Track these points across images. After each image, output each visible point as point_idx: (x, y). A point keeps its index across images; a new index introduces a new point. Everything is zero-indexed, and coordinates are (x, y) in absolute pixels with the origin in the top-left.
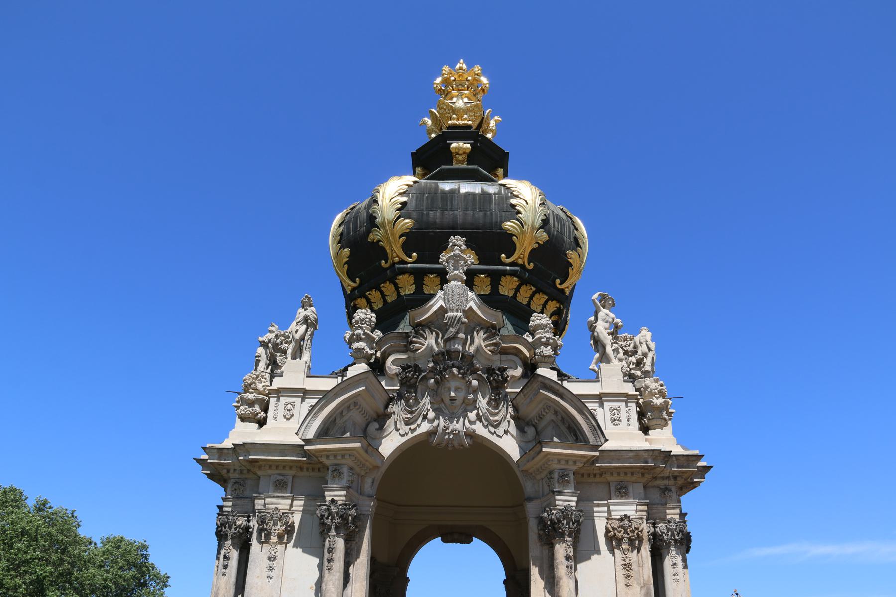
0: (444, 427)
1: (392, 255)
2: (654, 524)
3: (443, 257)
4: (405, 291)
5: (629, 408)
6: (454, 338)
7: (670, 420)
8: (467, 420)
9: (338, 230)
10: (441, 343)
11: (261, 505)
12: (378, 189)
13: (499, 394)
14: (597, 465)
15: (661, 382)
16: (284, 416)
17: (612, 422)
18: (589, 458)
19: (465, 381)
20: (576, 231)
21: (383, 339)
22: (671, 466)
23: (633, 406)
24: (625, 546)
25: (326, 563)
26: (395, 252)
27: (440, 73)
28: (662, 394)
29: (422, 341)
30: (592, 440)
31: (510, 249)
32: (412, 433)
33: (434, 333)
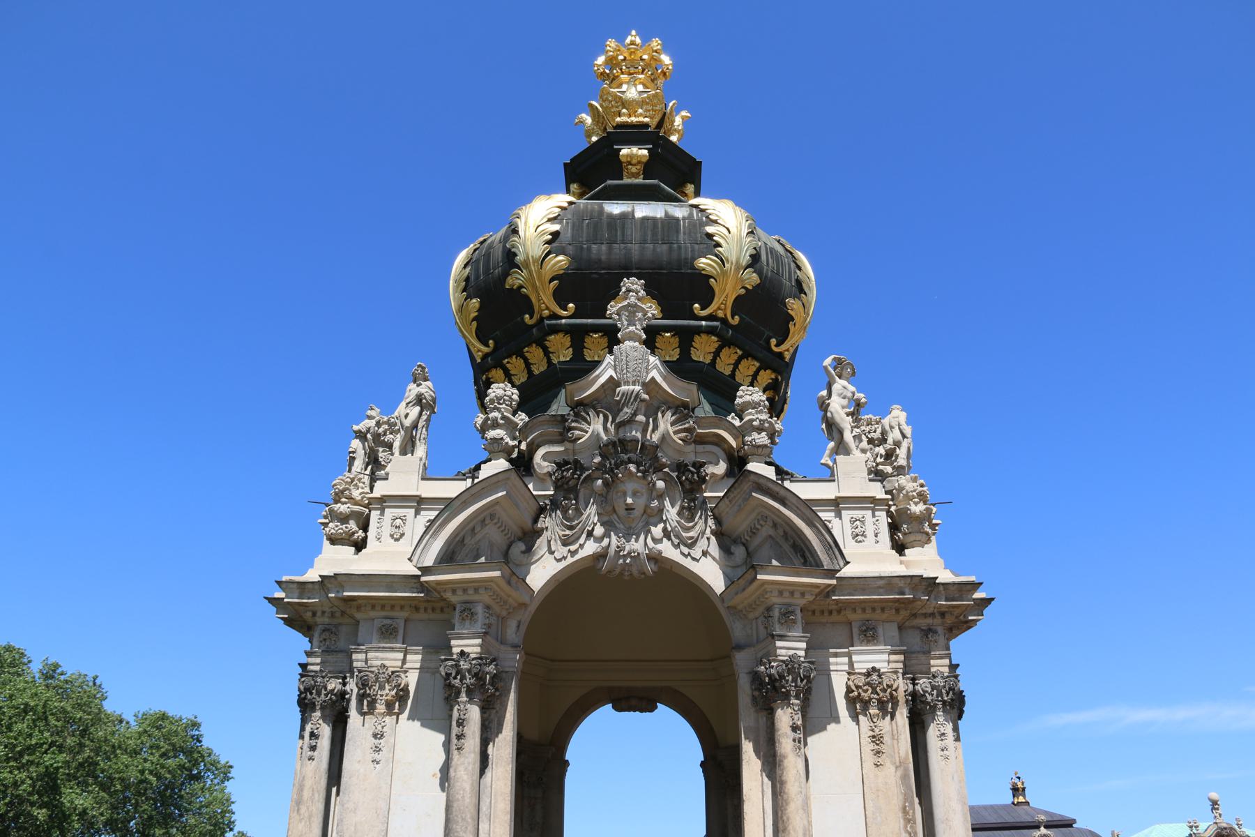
0: (618, 547)
1: (539, 306)
2: (913, 680)
3: (613, 308)
4: (559, 357)
5: (877, 518)
6: (630, 421)
7: (934, 534)
8: (649, 537)
9: (463, 272)
10: (612, 428)
11: (361, 661)
12: (519, 214)
13: (694, 500)
14: (833, 598)
15: (922, 481)
16: (392, 536)
17: (853, 538)
18: (822, 588)
19: (646, 483)
20: (798, 271)
21: (530, 425)
22: (937, 599)
23: (882, 515)
24: (873, 711)
25: (454, 741)
26: (544, 303)
27: (602, 50)
28: (922, 497)
29: (585, 426)
30: (826, 563)
31: (707, 296)
32: (572, 557)
33: (601, 415)
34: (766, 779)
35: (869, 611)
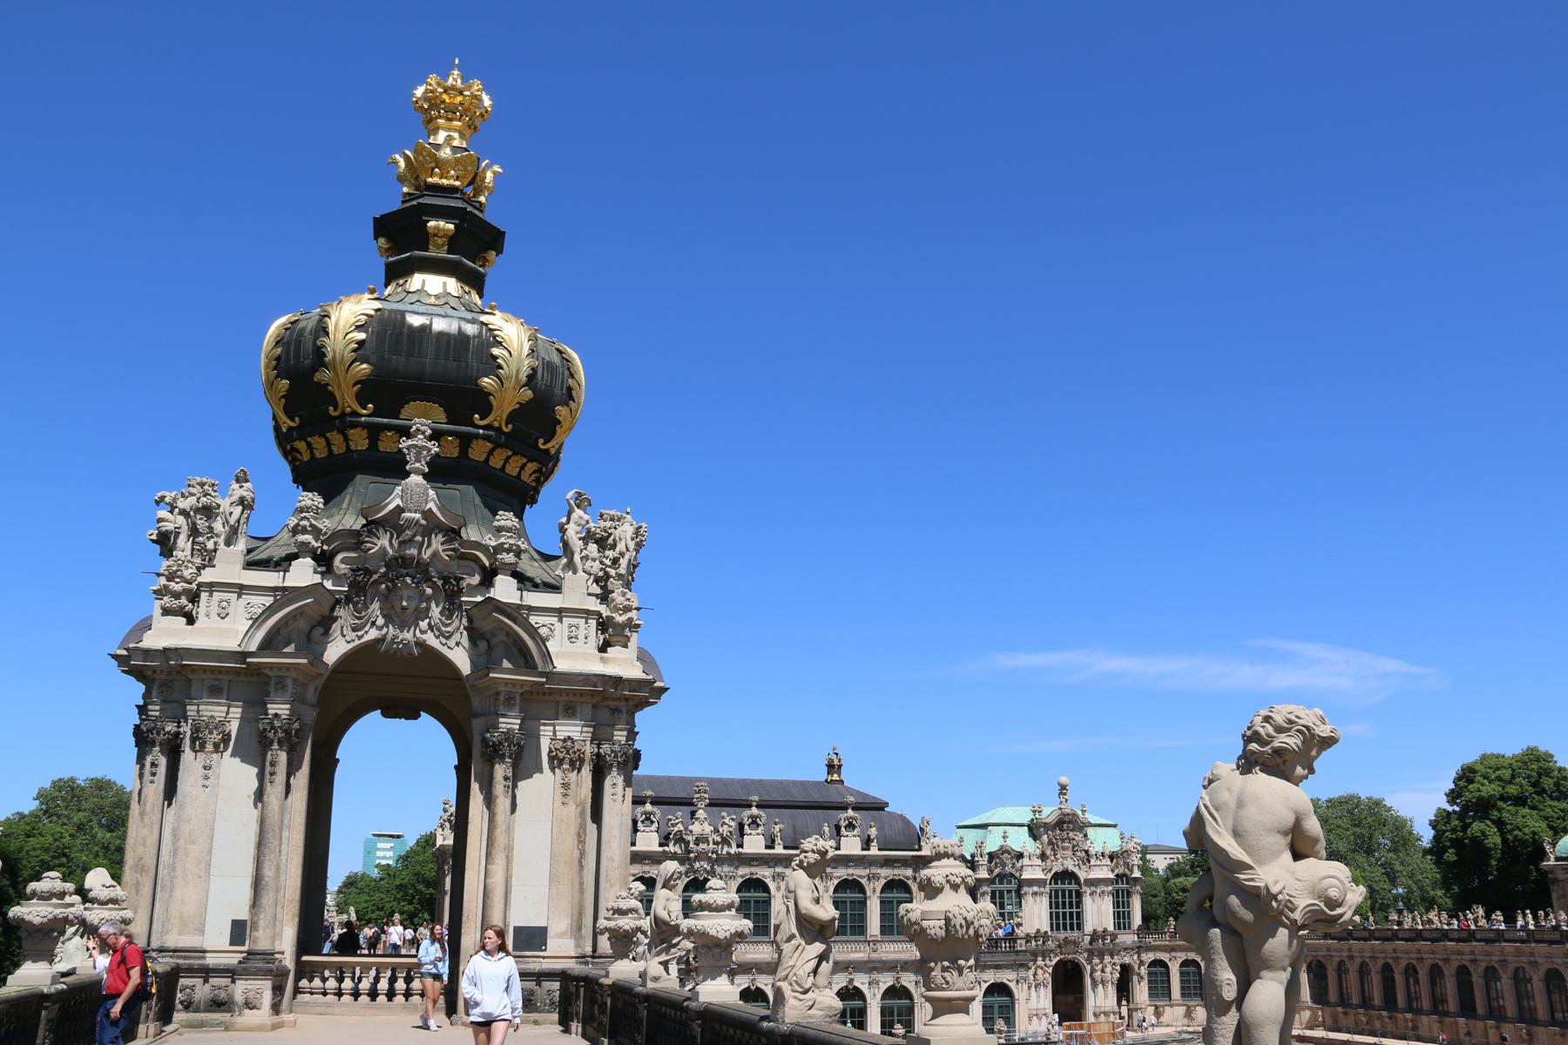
4: (356, 445)
8: (418, 632)
9: (274, 351)
11: (194, 711)
16: (219, 615)
24: (566, 766)
25: (268, 776)
27: (423, 81)
29: (375, 540)
31: (486, 410)
32: (359, 640)
34: (485, 810)
35: (571, 695)
